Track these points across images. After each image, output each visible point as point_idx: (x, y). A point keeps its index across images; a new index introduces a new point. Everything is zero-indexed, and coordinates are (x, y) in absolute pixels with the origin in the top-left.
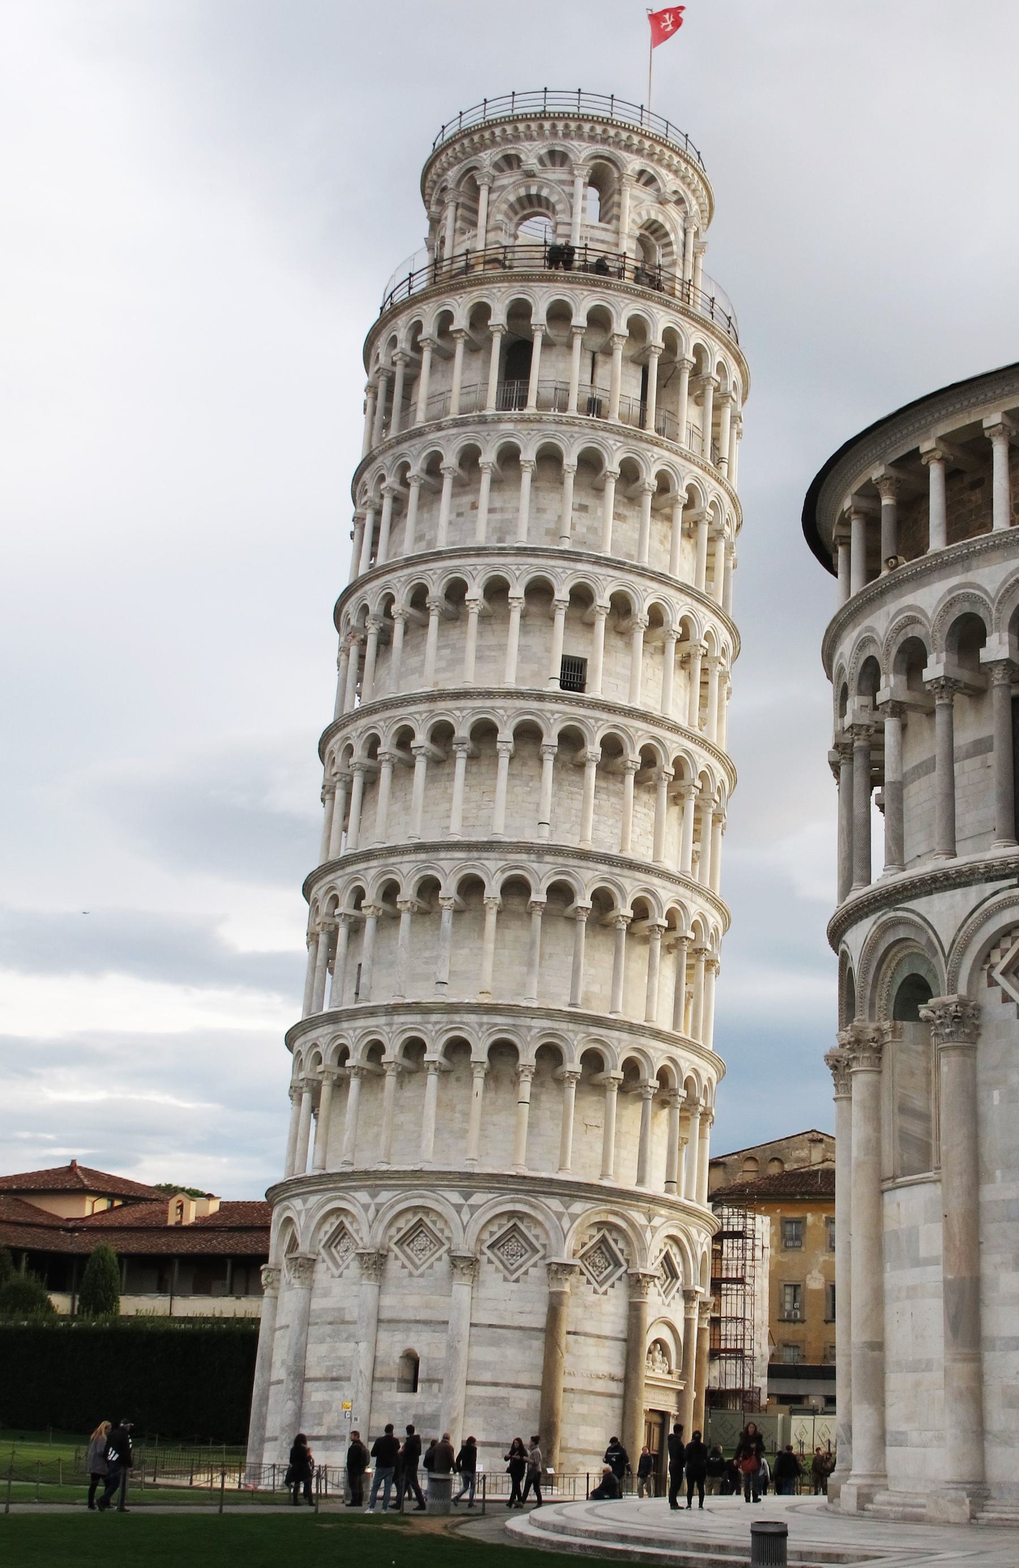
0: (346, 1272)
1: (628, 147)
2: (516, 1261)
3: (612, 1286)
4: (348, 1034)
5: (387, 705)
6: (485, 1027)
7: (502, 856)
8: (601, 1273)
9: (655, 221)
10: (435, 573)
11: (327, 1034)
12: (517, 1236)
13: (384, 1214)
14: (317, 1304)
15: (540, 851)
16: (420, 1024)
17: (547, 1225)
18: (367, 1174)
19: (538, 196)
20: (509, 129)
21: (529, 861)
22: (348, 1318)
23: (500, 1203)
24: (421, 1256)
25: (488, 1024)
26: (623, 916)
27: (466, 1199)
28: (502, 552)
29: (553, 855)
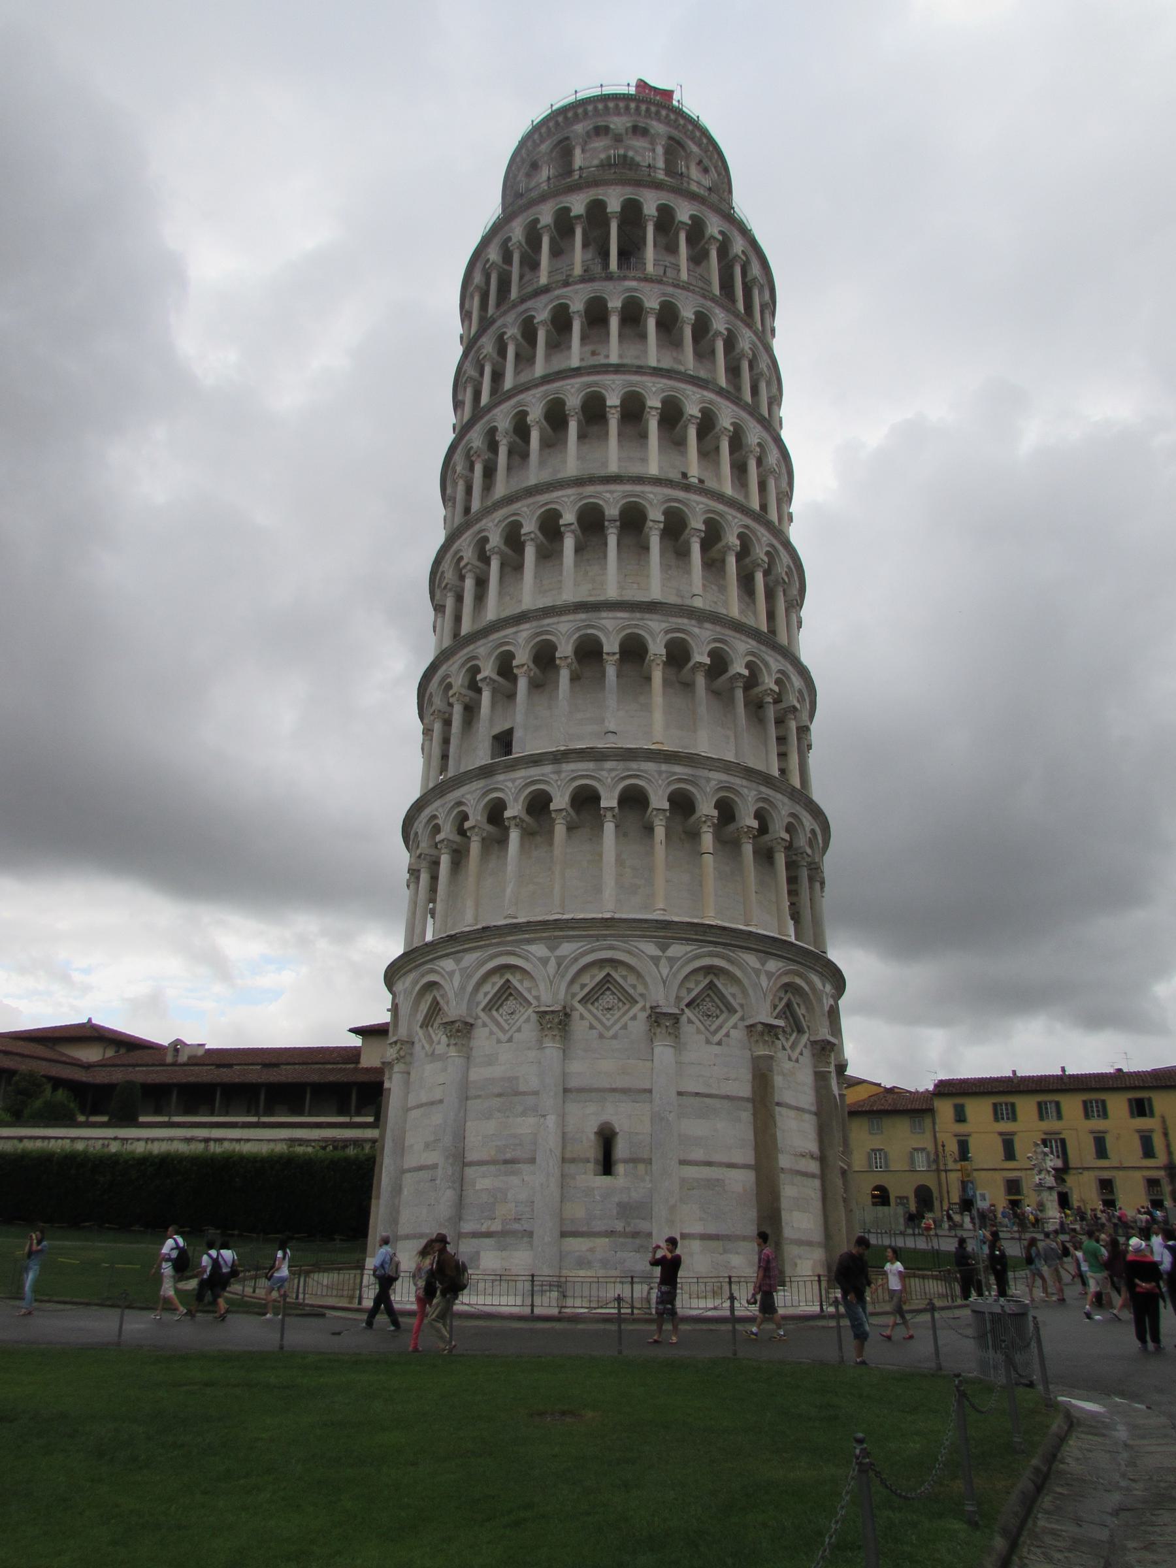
1: (692, 139)
3: (801, 1054)
4: (506, 786)
6: (664, 775)
7: (664, 618)
11: (477, 789)
12: (712, 995)
13: (567, 968)
14: (476, 1074)
16: (593, 770)
17: (745, 982)
19: (625, 156)
22: (522, 1088)
23: (697, 957)
24: (608, 1016)
25: (666, 772)
27: (664, 952)
28: (639, 370)
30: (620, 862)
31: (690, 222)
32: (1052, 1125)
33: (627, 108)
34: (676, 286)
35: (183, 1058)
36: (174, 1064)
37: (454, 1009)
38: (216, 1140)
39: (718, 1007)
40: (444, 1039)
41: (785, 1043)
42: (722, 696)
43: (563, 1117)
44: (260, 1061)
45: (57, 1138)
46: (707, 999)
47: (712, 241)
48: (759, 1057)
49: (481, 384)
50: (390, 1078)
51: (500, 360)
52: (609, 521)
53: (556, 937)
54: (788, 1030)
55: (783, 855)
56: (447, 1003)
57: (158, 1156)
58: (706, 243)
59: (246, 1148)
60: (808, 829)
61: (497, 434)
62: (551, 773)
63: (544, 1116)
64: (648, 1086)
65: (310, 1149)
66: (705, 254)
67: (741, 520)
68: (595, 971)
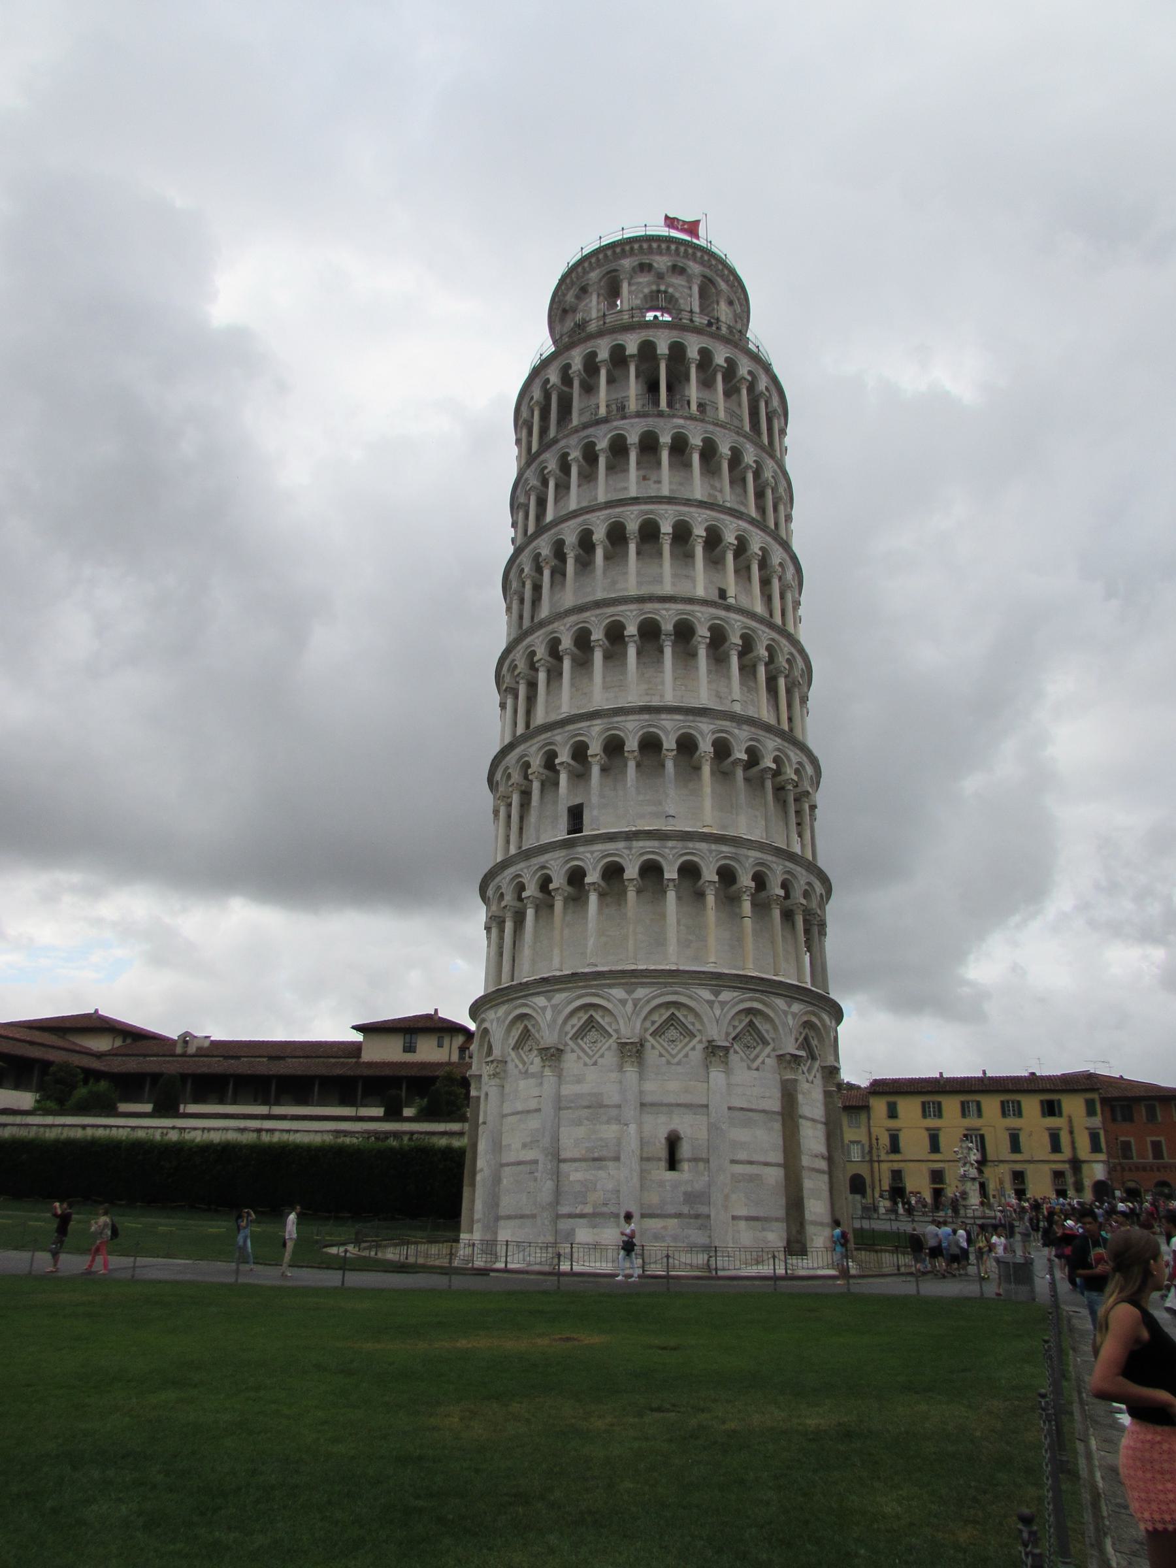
0: (600, 1061)
1: (722, 276)
3: (815, 1077)
6: (714, 854)
10: (632, 513)
12: (751, 1031)
13: (642, 1008)
16: (658, 848)
17: (777, 1021)
18: (623, 973)
20: (645, 246)
23: (742, 1001)
25: (715, 850)
27: (716, 997)
28: (688, 502)
29: (748, 725)
31: (725, 365)
32: (972, 1122)
33: (668, 248)
34: (716, 425)
35: (192, 1050)
36: (184, 1055)
37: (548, 1037)
38: (268, 1131)
39: (755, 1040)
40: (537, 1060)
42: (755, 783)
43: (640, 1125)
44: (265, 1054)
45: (118, 1127)
47: (743, 381)
48: (787, 1080)
52: (666, 635)
53: (632, 984)
55: (801, 917)
57: (219, 1144)
58: (738, 381)
59: (298, 1138)
60: (818, 894)
61: (565, 547)
62: (624, 848)
63: (627, 1125)
65: (355, 1140)
66: (737, 391)
67: (769, 635)
68: (663, 1011)
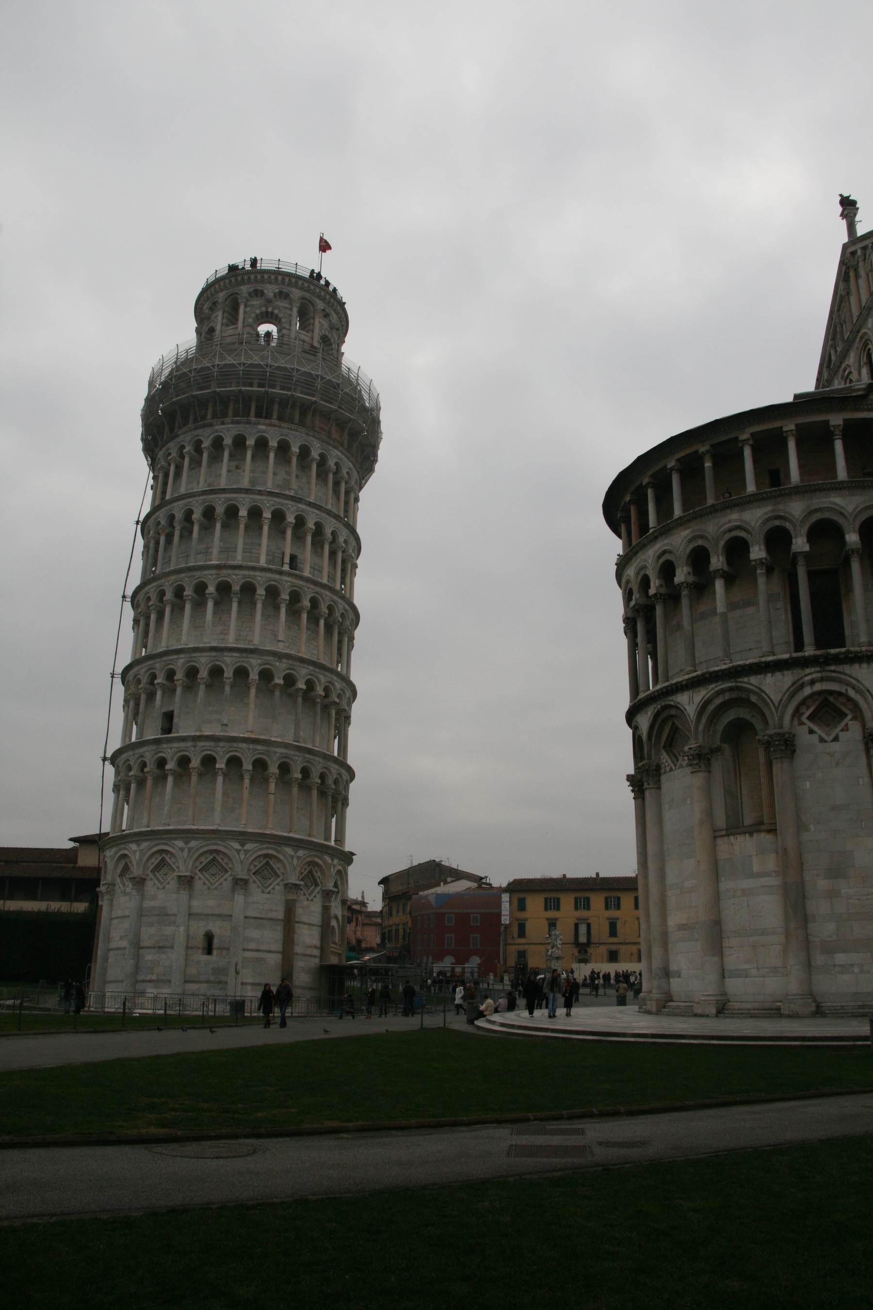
0: (167, 886)
1: (319, 297)
2: (267, 882)
3: (315, 897)
5: (190, 569)
6: (251, 751)
8: (309, 889)
9: (327, 336)
10: (220, 500)
12: (268, 868)
14: (147, 904)
15: (279, 656)
17: (285, 862)
19: (272, 313)
21: (274, 661)
23: (260, 849)
24: (213, 878)
26: (320, 695)
28: (260, 493)
30: (225, 794)
37: (136, 871)
40: (130, 885)
41: (305, 892)
46: (265, 870)
48: (289, 900)
49: (169, 470)
50: (102, 900)
51: (181, 460)
52: (234, 594)
54: (310, 884)
56: (133, 865)
61: (175, 521)
64: (230, 913)
